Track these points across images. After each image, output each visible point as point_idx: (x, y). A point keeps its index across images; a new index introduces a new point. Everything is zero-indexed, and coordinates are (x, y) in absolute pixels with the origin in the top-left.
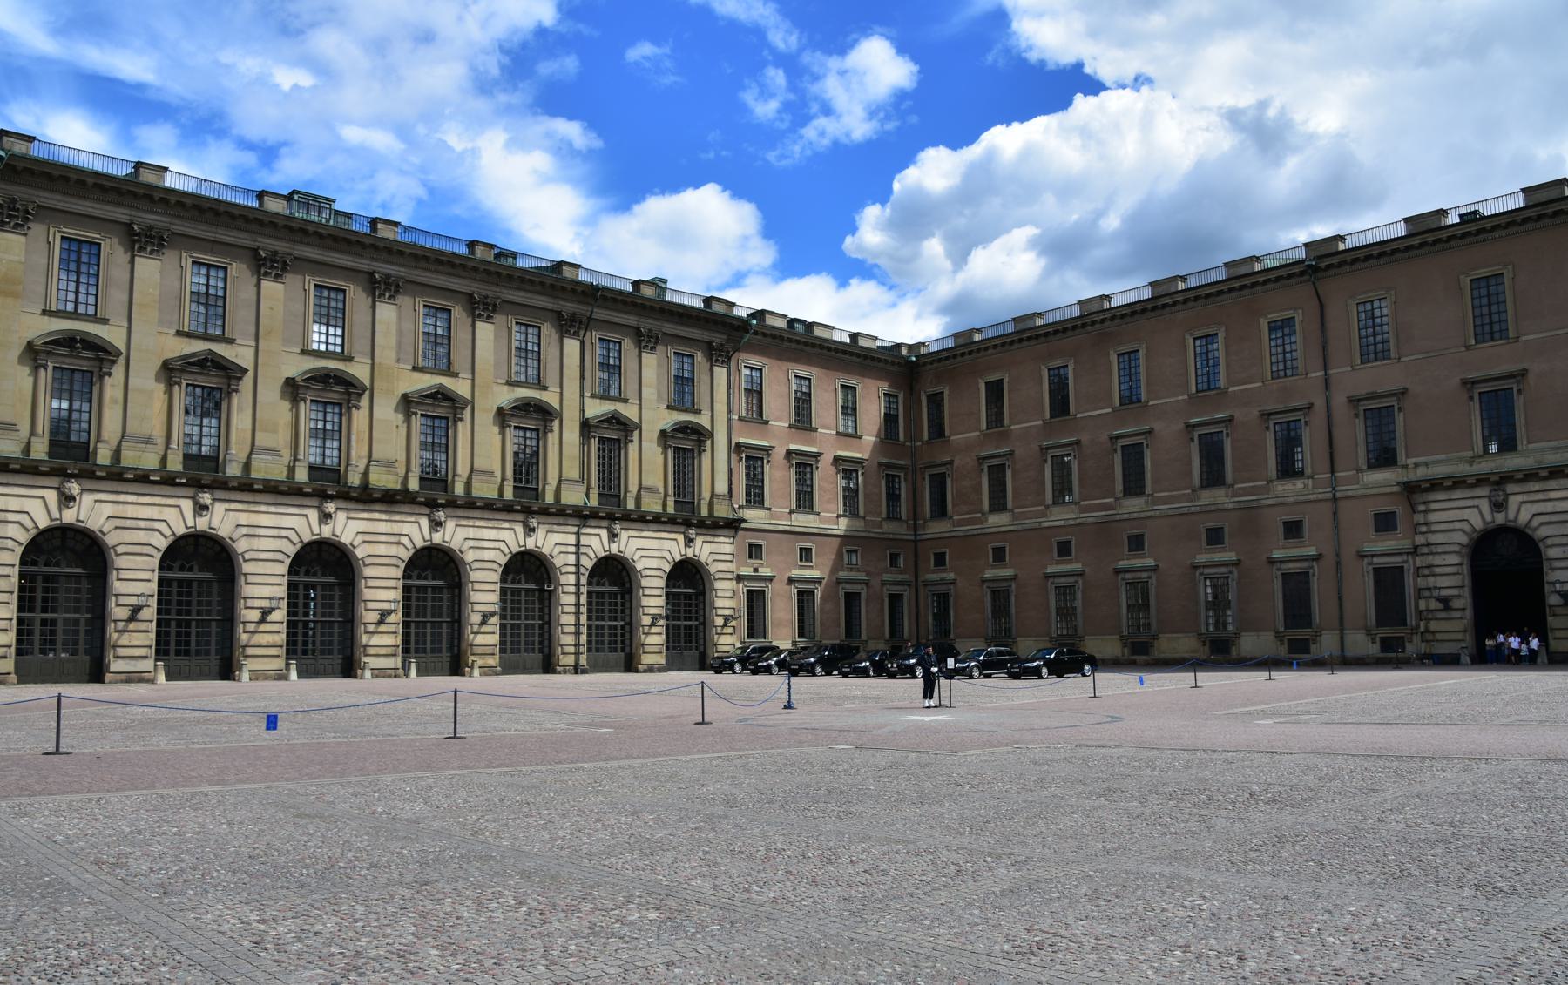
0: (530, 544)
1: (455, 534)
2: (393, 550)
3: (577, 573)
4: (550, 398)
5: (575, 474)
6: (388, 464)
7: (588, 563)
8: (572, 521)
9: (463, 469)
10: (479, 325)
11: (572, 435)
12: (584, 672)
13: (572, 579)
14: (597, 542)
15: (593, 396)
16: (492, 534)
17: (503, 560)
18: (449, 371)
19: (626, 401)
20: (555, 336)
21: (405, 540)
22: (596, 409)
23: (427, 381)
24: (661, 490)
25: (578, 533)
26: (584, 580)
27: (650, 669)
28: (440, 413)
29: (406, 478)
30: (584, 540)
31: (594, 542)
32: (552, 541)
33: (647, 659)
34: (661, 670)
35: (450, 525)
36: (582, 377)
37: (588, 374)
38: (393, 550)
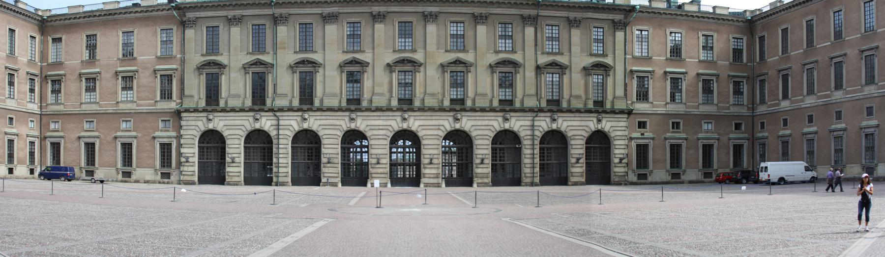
0: (507, 126)
1: (467, 123)
2: (436, 132)
3: (533, 140)
4: (517, 57)
5: (533, 92)
6: (433, 95)
7: (539, 134)
8: (529, 114)
9: (471, 93)
10: (478, 27)
11: (530, 74)
12: (536, 185)
13: (529, 142)
14: (544, 124)
15: (543, 53)
16: (486, 123)
17: (492, 135)
18: (464, 50)
19: (562, 54)
20: (519, 29)
21: (442, 128)
22: (543, 60)
23: (452, 56)
24: (583, 97)
25: (533, 120)
26: (537, 142)
27: (576, 184)
28: (459, 69)
29: (442, 101)
30: (536, 123)
31: (543, 124)
32: (518, 124)
33: (573, 179)
34: (582, 184)
35: (464, 120)
36: (536, 45)
37: (539, 43)
38: (436, 132)
